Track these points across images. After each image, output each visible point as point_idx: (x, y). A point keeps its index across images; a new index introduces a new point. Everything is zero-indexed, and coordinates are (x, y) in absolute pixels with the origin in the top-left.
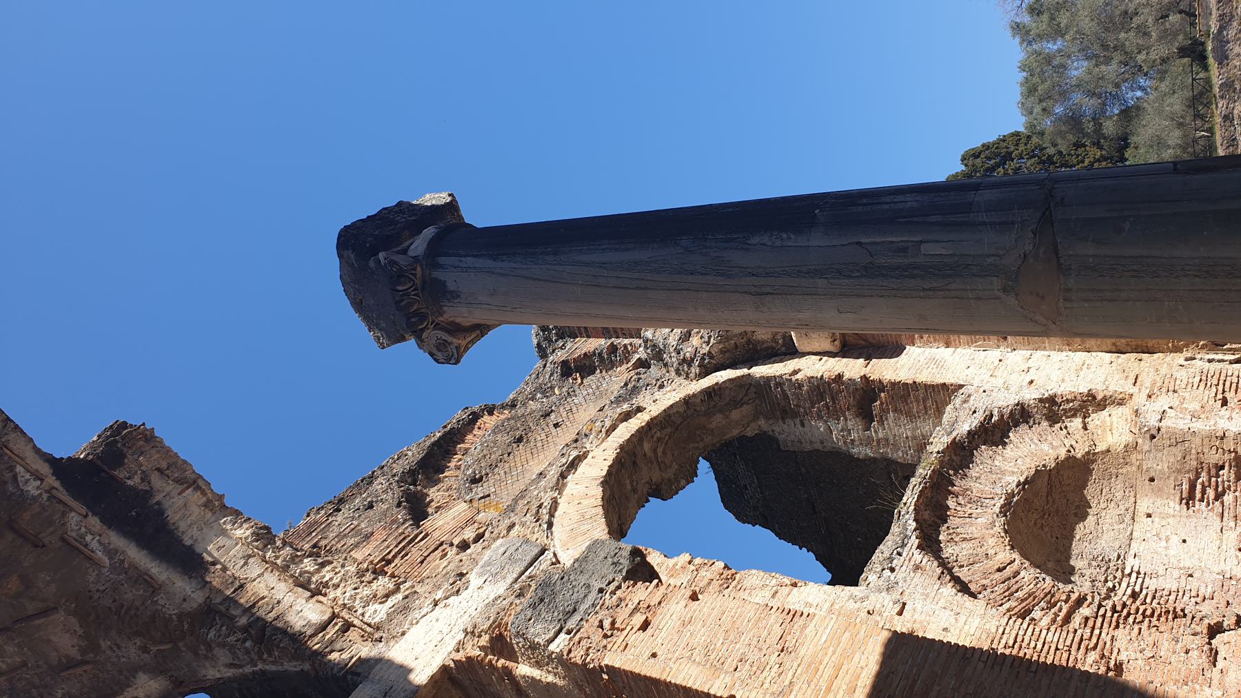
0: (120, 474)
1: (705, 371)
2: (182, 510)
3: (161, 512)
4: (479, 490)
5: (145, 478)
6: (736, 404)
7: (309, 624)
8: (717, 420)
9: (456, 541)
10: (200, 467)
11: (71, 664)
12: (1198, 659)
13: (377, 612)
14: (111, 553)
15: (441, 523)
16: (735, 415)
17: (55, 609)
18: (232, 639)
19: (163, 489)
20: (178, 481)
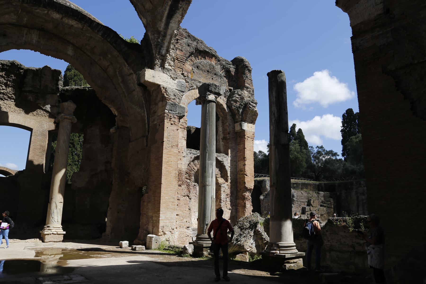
0: (181, 2)
1: (228, 106)
2: (178, 16)
3: (175, 14)
4: (195, 70)
5: (181, 7)
6: (223, 113)
7: (162, 53)
8: (220, 110)
9: (183, 72)
10: (186, 16)
11: (144, 7)
12: (184, 195)
13: (167, 66)
14: (165, 9)
15: (187, 66)
16: (221, 113)
17: (152, 4)
18: (156, 40)
19: (180, 12)
20: (182, 13)
